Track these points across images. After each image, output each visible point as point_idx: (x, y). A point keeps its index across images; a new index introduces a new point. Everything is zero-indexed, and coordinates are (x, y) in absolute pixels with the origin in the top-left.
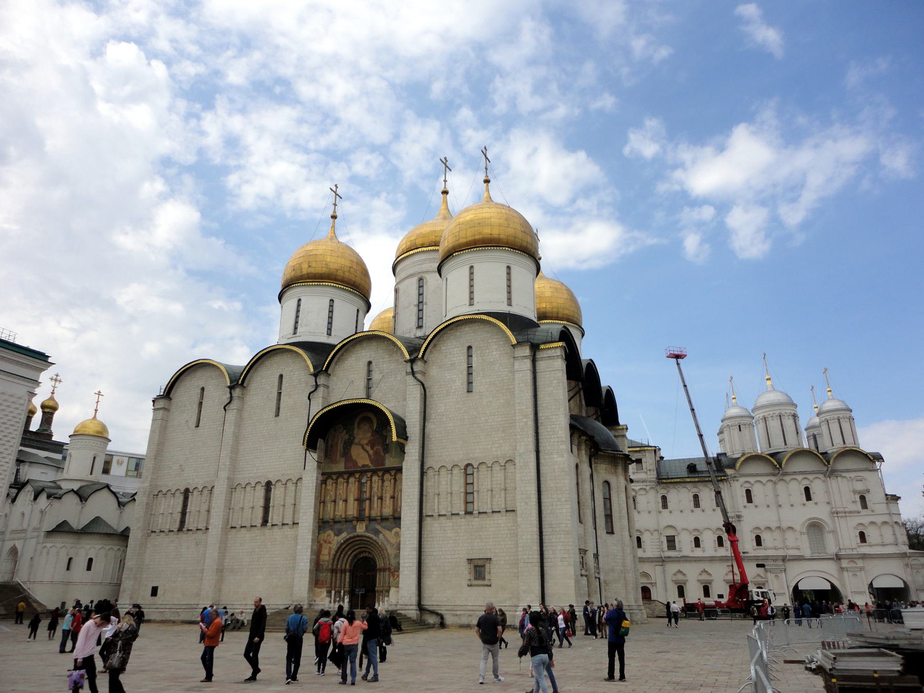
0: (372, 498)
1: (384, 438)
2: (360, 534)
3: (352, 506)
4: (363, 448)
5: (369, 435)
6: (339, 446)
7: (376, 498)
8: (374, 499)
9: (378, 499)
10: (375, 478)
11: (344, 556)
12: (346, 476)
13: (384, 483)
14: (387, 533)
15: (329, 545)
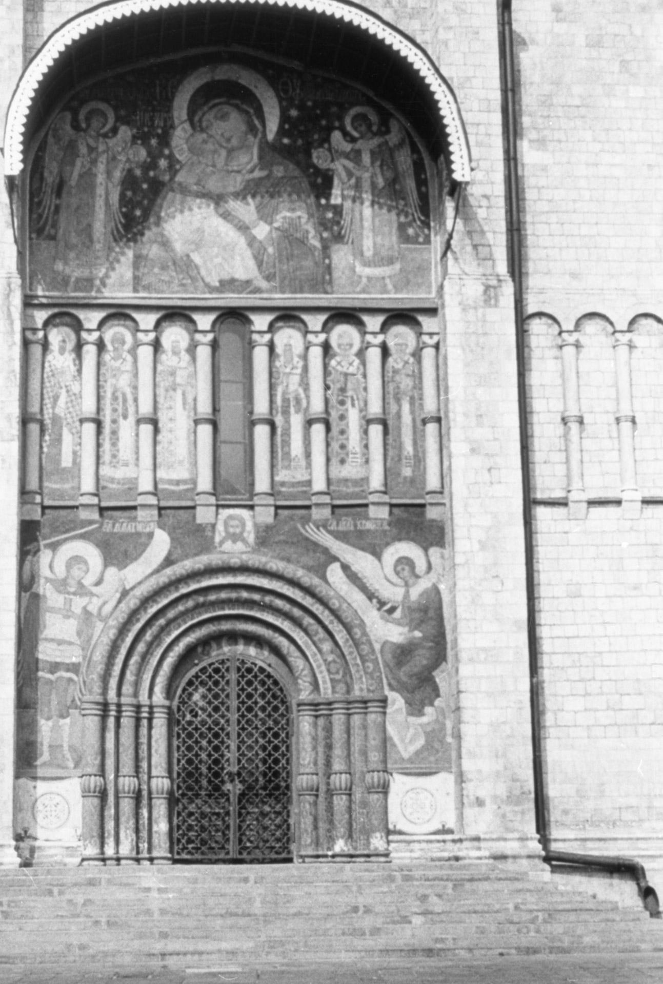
0: (279, 420)
1: (319, 180)
2: (235, 561)
3: (181, 449)
4: (226, 216)
5: (248, 159)
6: (100, 191)
7: (297, 421)
8: (287, 421)
9: (309, 423)
10: (288, 337)
11: (150, 646)
12: (147, 320)
13: (333, 363)
14: (362, 562)
15: (78, 603)
